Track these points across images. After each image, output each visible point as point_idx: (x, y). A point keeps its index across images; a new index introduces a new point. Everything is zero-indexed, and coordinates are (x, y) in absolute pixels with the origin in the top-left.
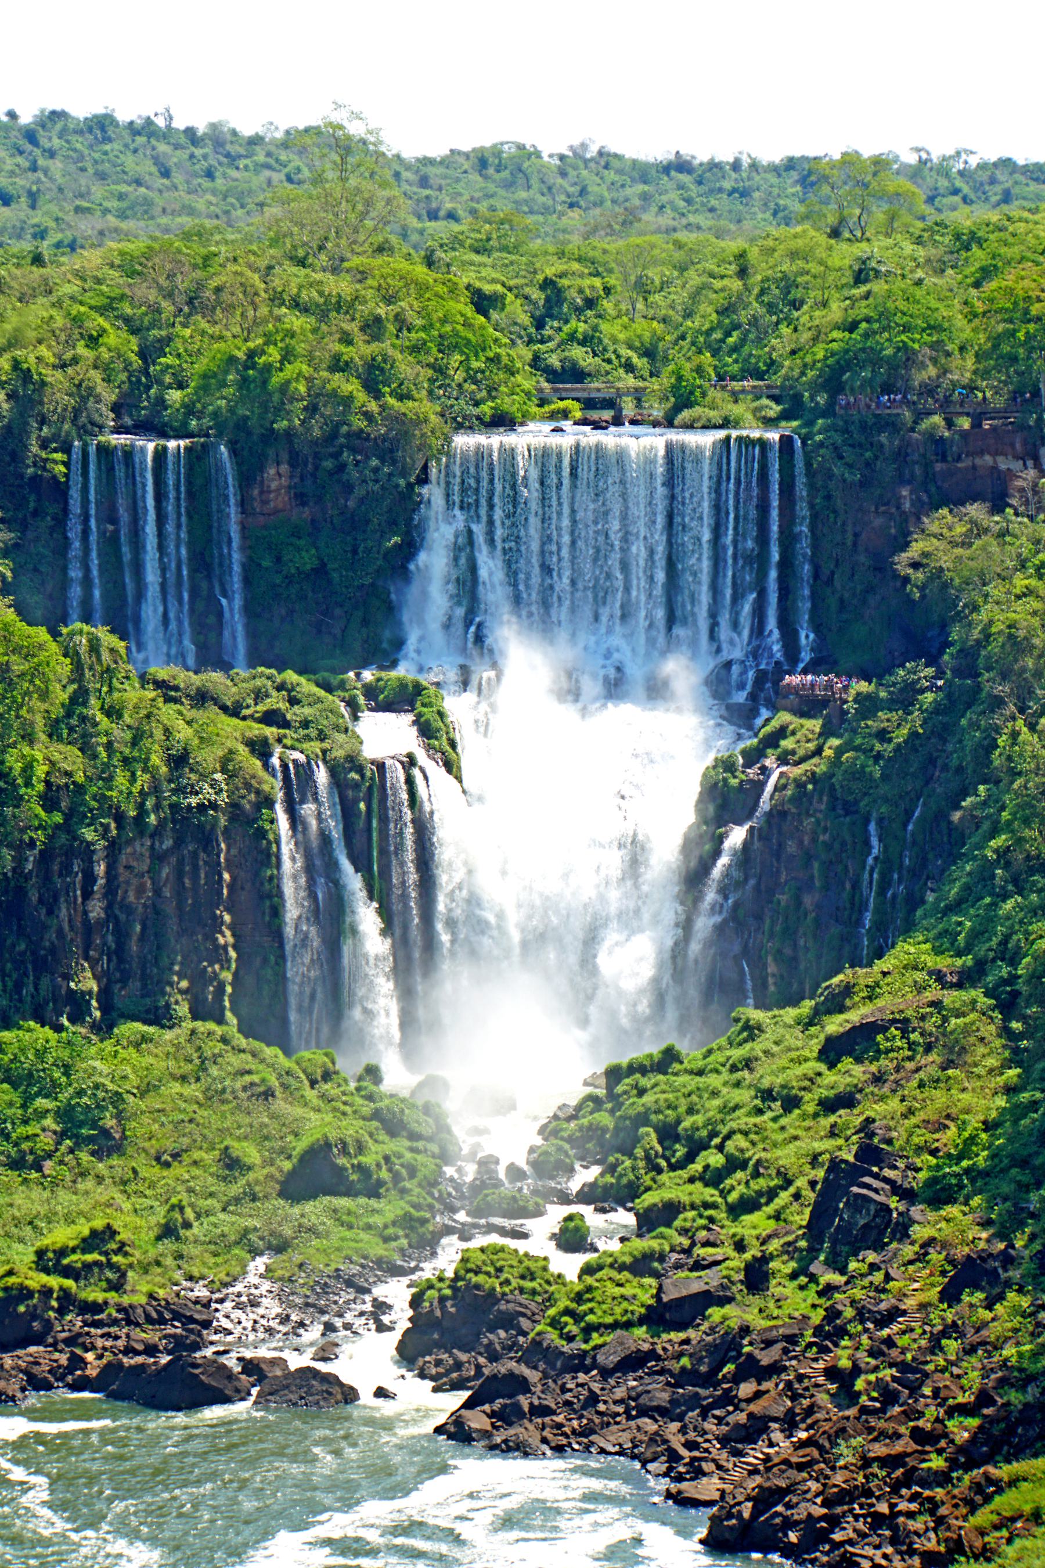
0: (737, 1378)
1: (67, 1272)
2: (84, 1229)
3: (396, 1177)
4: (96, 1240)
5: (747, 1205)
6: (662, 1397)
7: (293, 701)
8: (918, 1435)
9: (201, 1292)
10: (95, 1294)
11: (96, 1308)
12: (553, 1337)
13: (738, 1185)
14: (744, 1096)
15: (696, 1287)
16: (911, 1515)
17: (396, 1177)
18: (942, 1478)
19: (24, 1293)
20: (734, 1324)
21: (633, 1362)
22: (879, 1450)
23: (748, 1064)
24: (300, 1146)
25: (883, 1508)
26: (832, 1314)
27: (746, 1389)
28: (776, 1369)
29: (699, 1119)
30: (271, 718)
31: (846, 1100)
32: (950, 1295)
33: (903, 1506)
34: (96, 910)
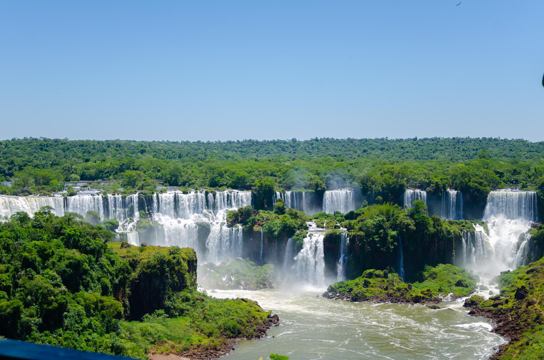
0: (500, 314)
1: (424, 294)
2: (426, 289)
3: (470, 285)
4: (428, 290)
5: (513, 291)
6: (491, 316)
7: (466, 224)
8: (517, 324)
9: (442, 298)
10: (427, 297)
11: (427, 299)
12: (480, 307)
13: (513, 289)
14: (516, 277)
15: (498, 302)
16: (513, 334)
17: (470, 285)
18: (518, 330)
19: (417, 296)
20: (501, 308)
21: (489, 311)
22: (511, 326)
23: (518, 273)
24: (457, 280)
25: (510, 333)
26: (513, 307)
27: (500, 316)
28: (505, 314)
29: (511, 279)
30: (463, 226)
31: (528, 279)
32: (527, 307)
33: (513, 333)
34: (436, 250)
